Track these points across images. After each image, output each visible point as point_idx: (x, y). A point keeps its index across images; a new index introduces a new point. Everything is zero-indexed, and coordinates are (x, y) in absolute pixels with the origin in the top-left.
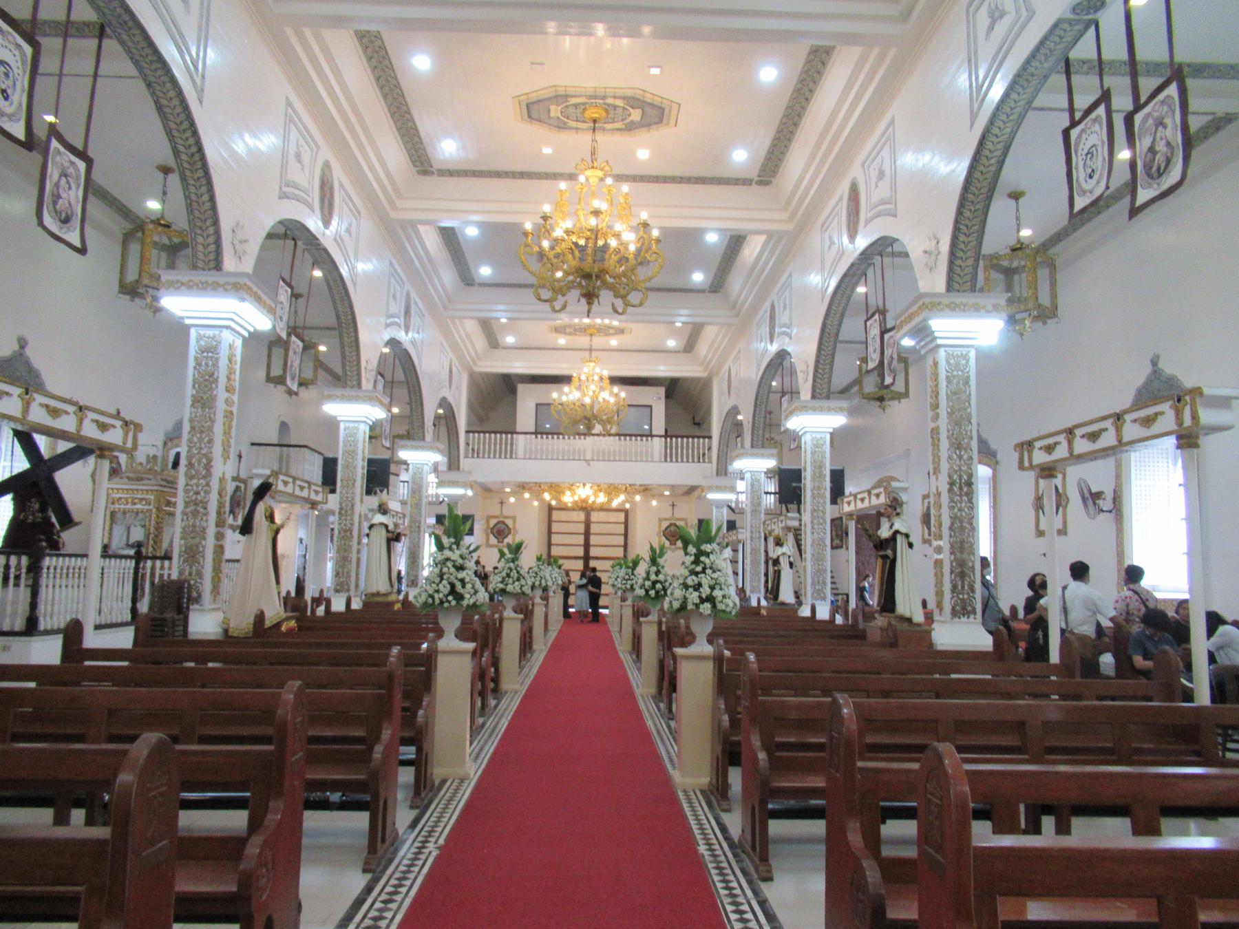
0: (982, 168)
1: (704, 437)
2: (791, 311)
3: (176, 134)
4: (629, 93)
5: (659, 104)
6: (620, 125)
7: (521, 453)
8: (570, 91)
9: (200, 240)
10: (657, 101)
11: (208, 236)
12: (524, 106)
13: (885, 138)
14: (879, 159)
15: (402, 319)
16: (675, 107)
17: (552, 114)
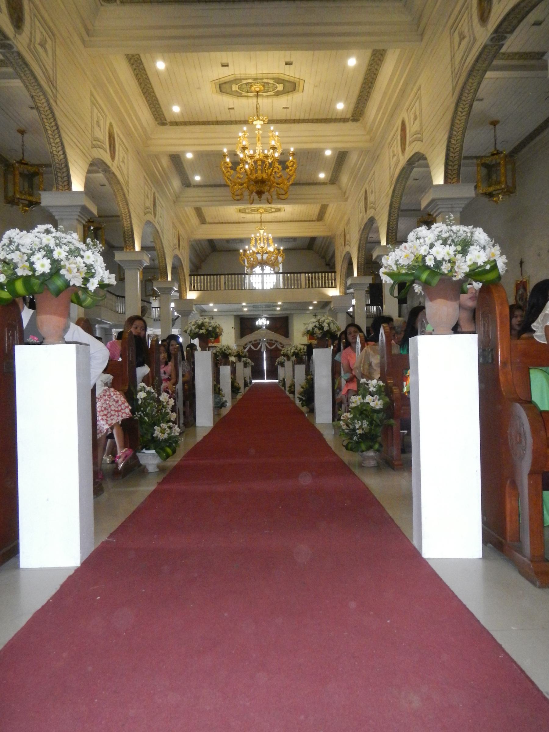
0: (459, 117)
1: (331, 272)
2: (375, 194)
3: (45, 120)
4: (275, 76)
5: (292, 81)
6: (272, 93)
7: (223, 287)
8: (243, 76)
9: (59, 174)
10: (292, 79)
11: (63, 173)
12: (218, 86)
13: (416, 97)
14: (414, 108)
15: (152, 209)
16: (302, 82)
17: (234, 89)
